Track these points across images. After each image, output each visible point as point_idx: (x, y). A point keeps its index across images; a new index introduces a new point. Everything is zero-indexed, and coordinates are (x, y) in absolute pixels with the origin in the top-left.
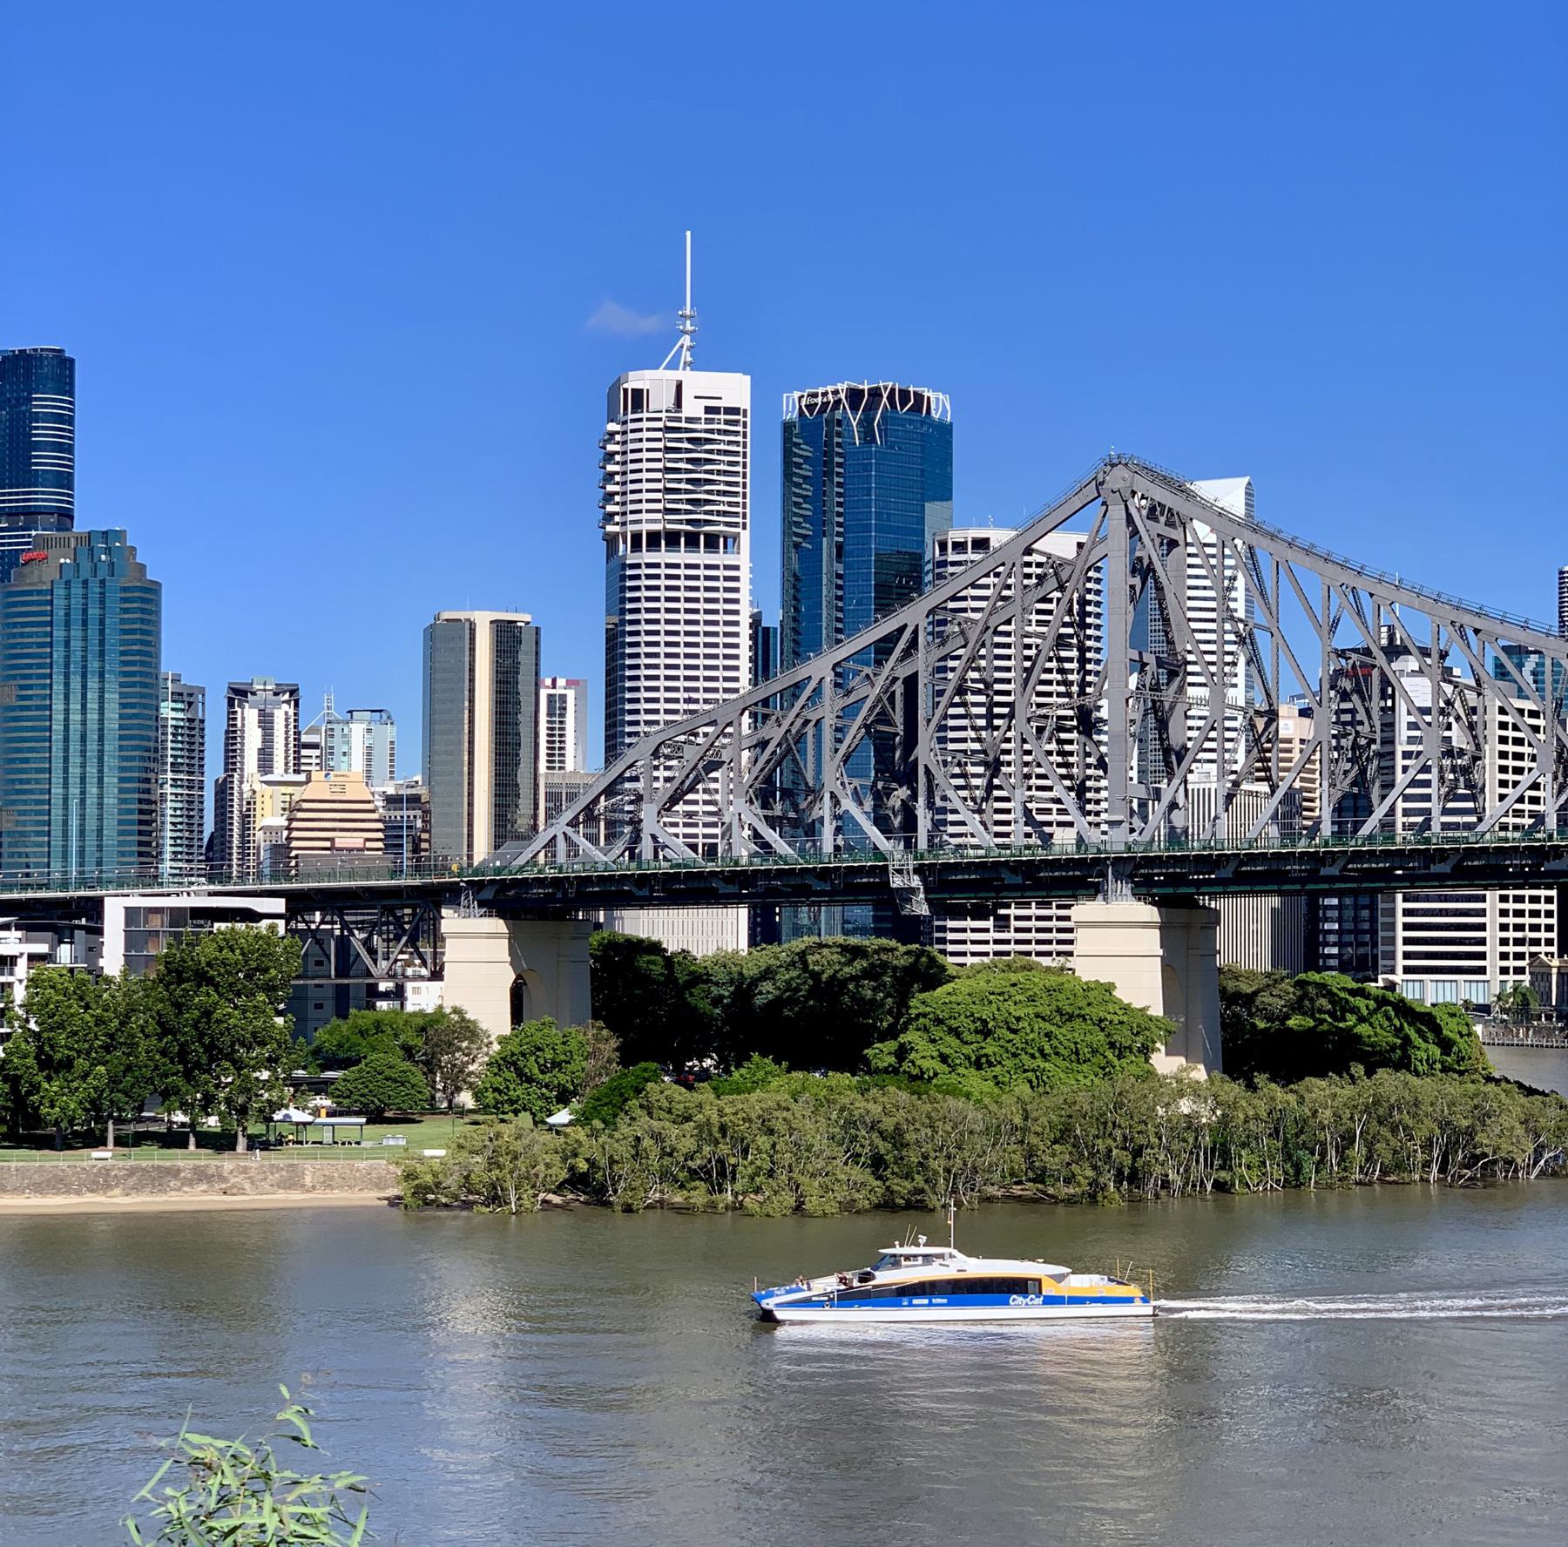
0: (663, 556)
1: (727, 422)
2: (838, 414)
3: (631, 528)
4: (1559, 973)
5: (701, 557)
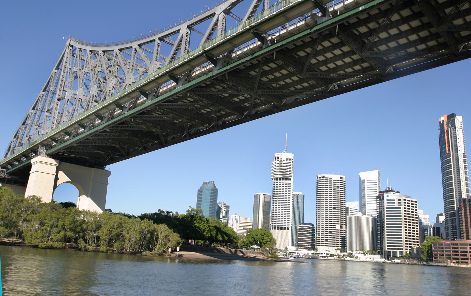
0: (279, 181)
4: (416, 250)
5: (285, 181)
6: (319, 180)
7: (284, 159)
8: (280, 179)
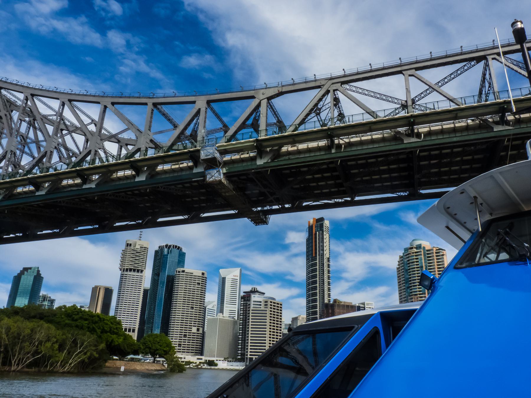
0: (129, 273)
1: (144, 250)
3: (124, 267)
5: (136, 274)
6: (178, 275)
7: (138, 247)
8: (131, 270)
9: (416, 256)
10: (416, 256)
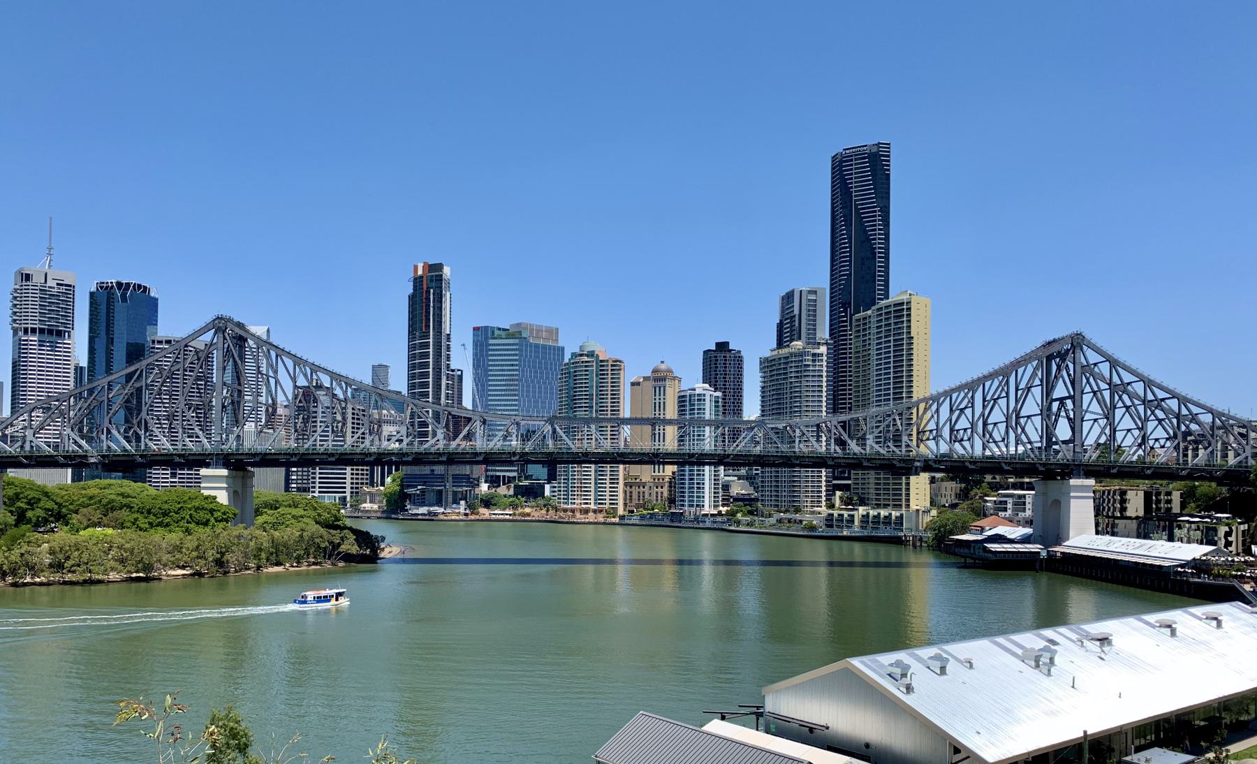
1: (66, 290)
2: (112, 291)
7: (51, 283)
9: (586, 366)
10: (586, 366)
